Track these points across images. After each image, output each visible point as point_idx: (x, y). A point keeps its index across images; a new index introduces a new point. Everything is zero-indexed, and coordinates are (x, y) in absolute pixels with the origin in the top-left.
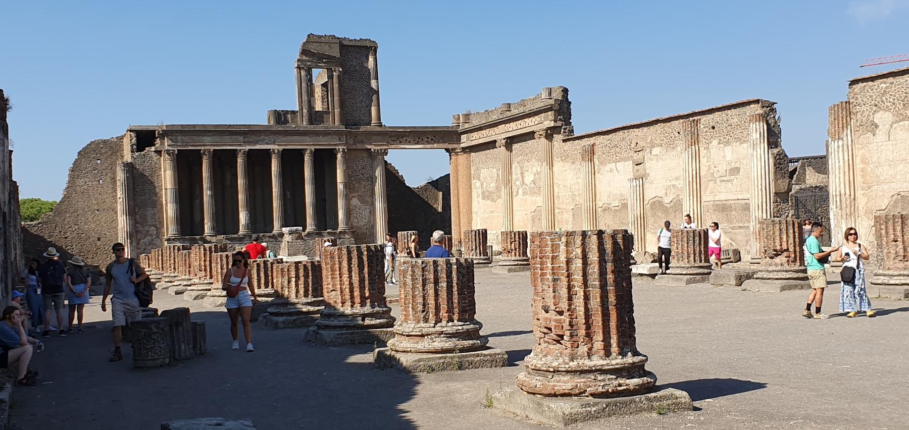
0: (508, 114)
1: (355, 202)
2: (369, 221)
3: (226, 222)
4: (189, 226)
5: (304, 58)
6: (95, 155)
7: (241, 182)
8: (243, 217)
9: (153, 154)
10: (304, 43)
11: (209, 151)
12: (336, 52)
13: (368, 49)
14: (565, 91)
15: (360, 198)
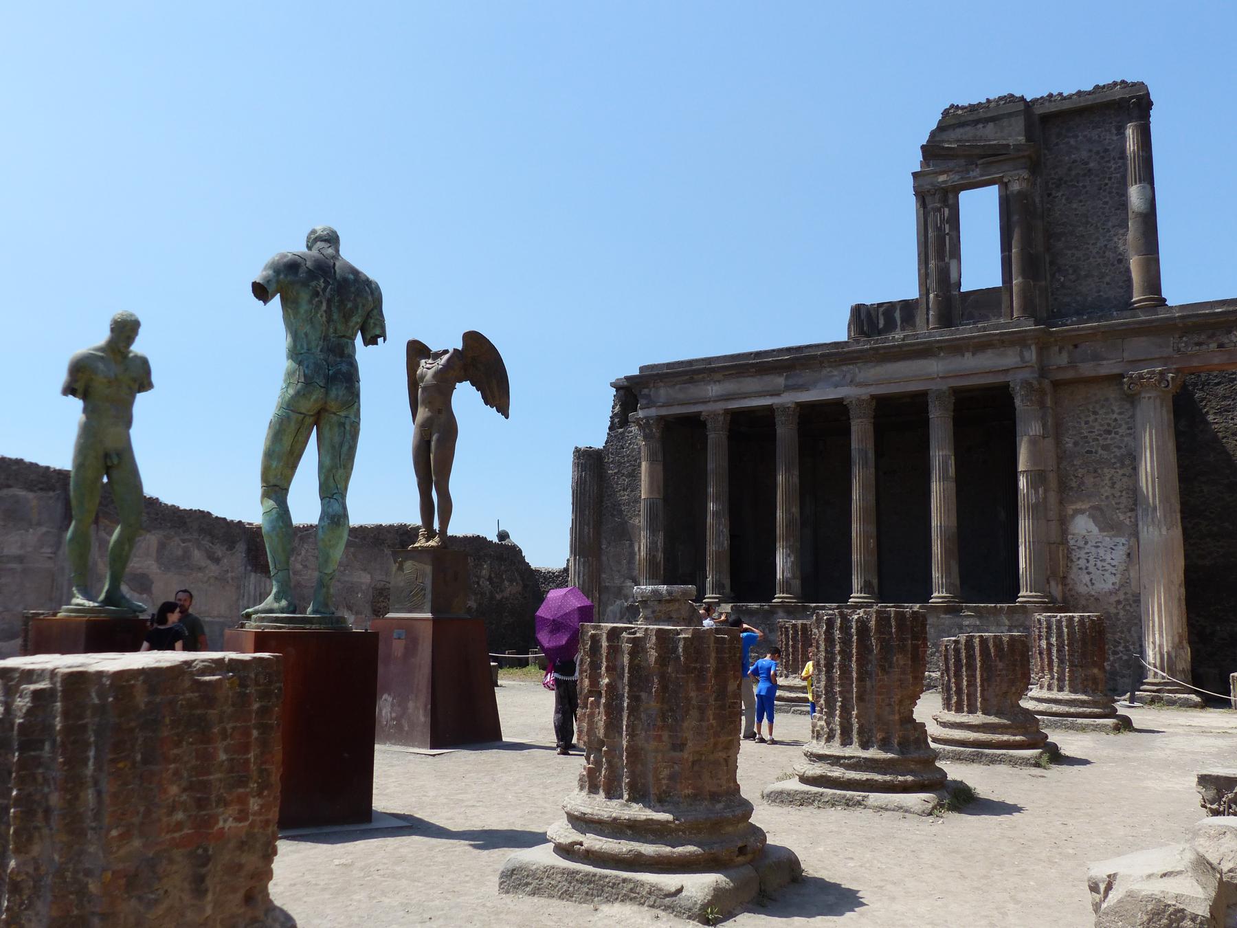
2: (1125, 583)
8: (782, 563)
10: (933, 134)
11: (715, 415)
12: (1014, 135)
13: (1126, 106)
15: (1099, 515)
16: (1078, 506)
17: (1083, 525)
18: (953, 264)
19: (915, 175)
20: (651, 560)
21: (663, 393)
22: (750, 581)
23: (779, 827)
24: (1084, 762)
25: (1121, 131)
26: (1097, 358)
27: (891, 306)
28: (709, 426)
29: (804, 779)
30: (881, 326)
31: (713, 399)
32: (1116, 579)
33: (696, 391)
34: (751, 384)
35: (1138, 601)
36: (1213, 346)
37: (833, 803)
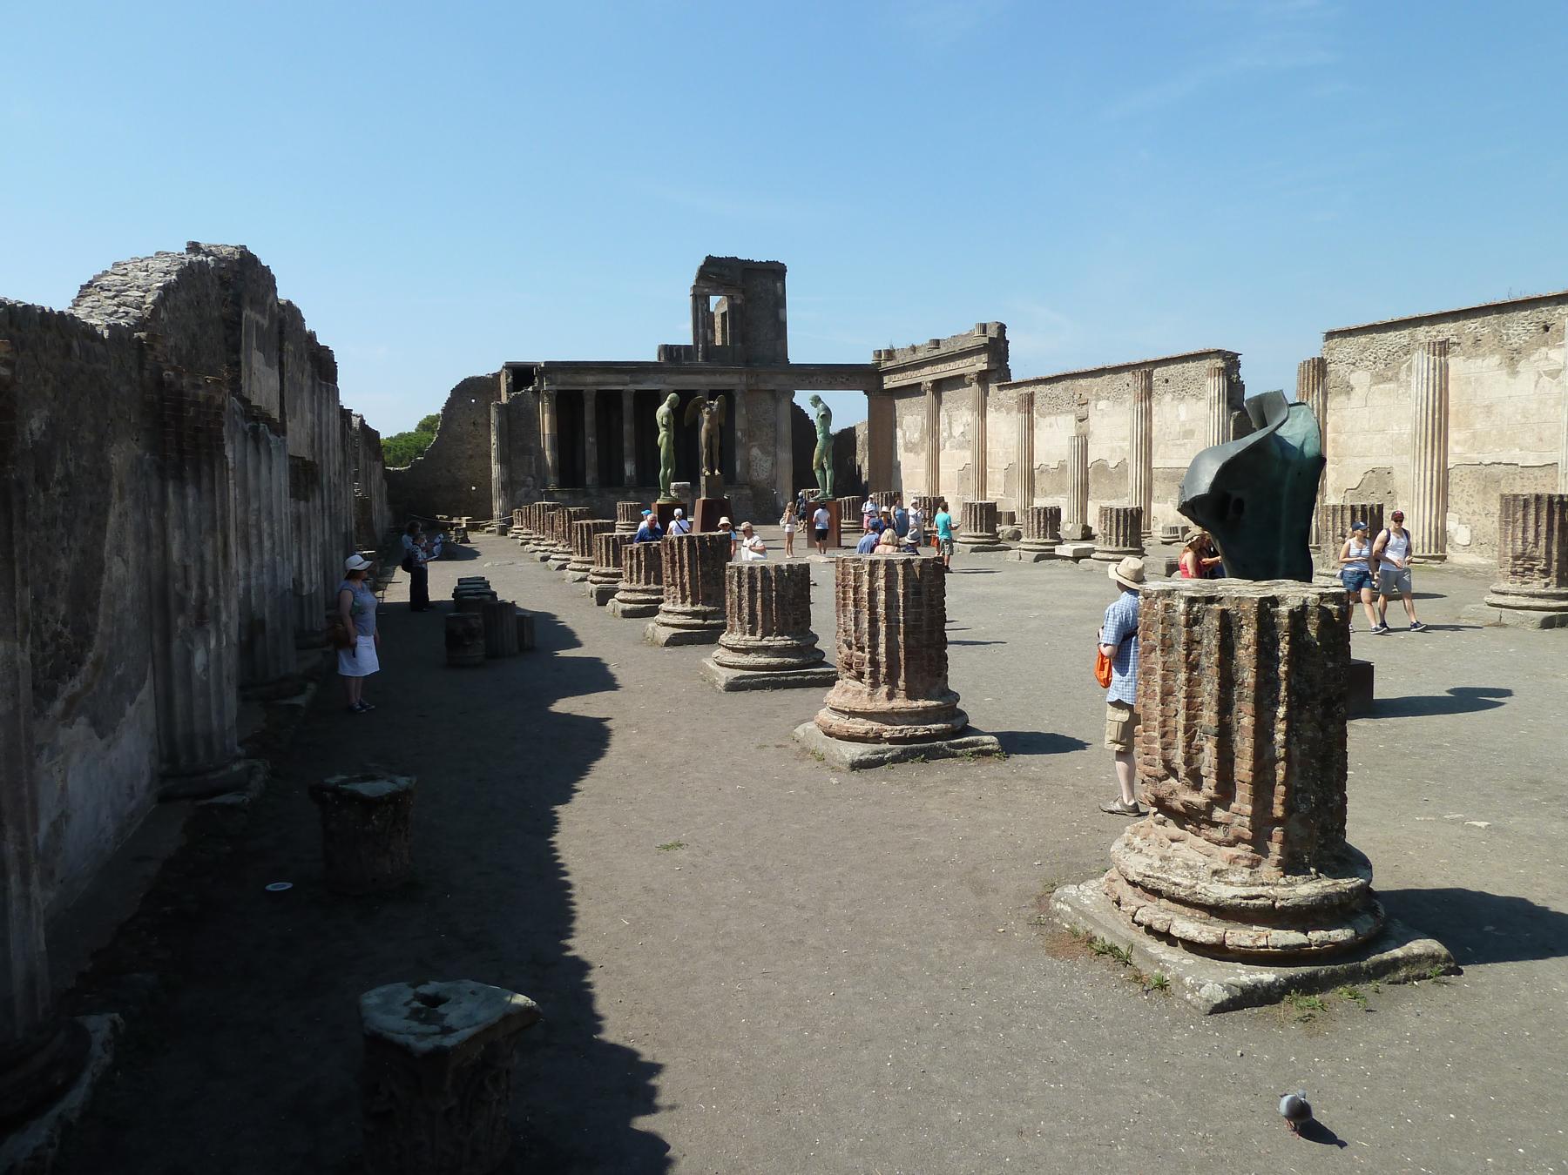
0: (936, 352)
1: (755, 452)
4: (569, 474)
6: (471, 392)
8: (629, 469)
13: (776, 272)
14: (1002, 328)
17: (755, 452)
21: (560, 377)
25: (774, 282)
31: (590, 382)
33: (579, 378)
34: (611, 378)
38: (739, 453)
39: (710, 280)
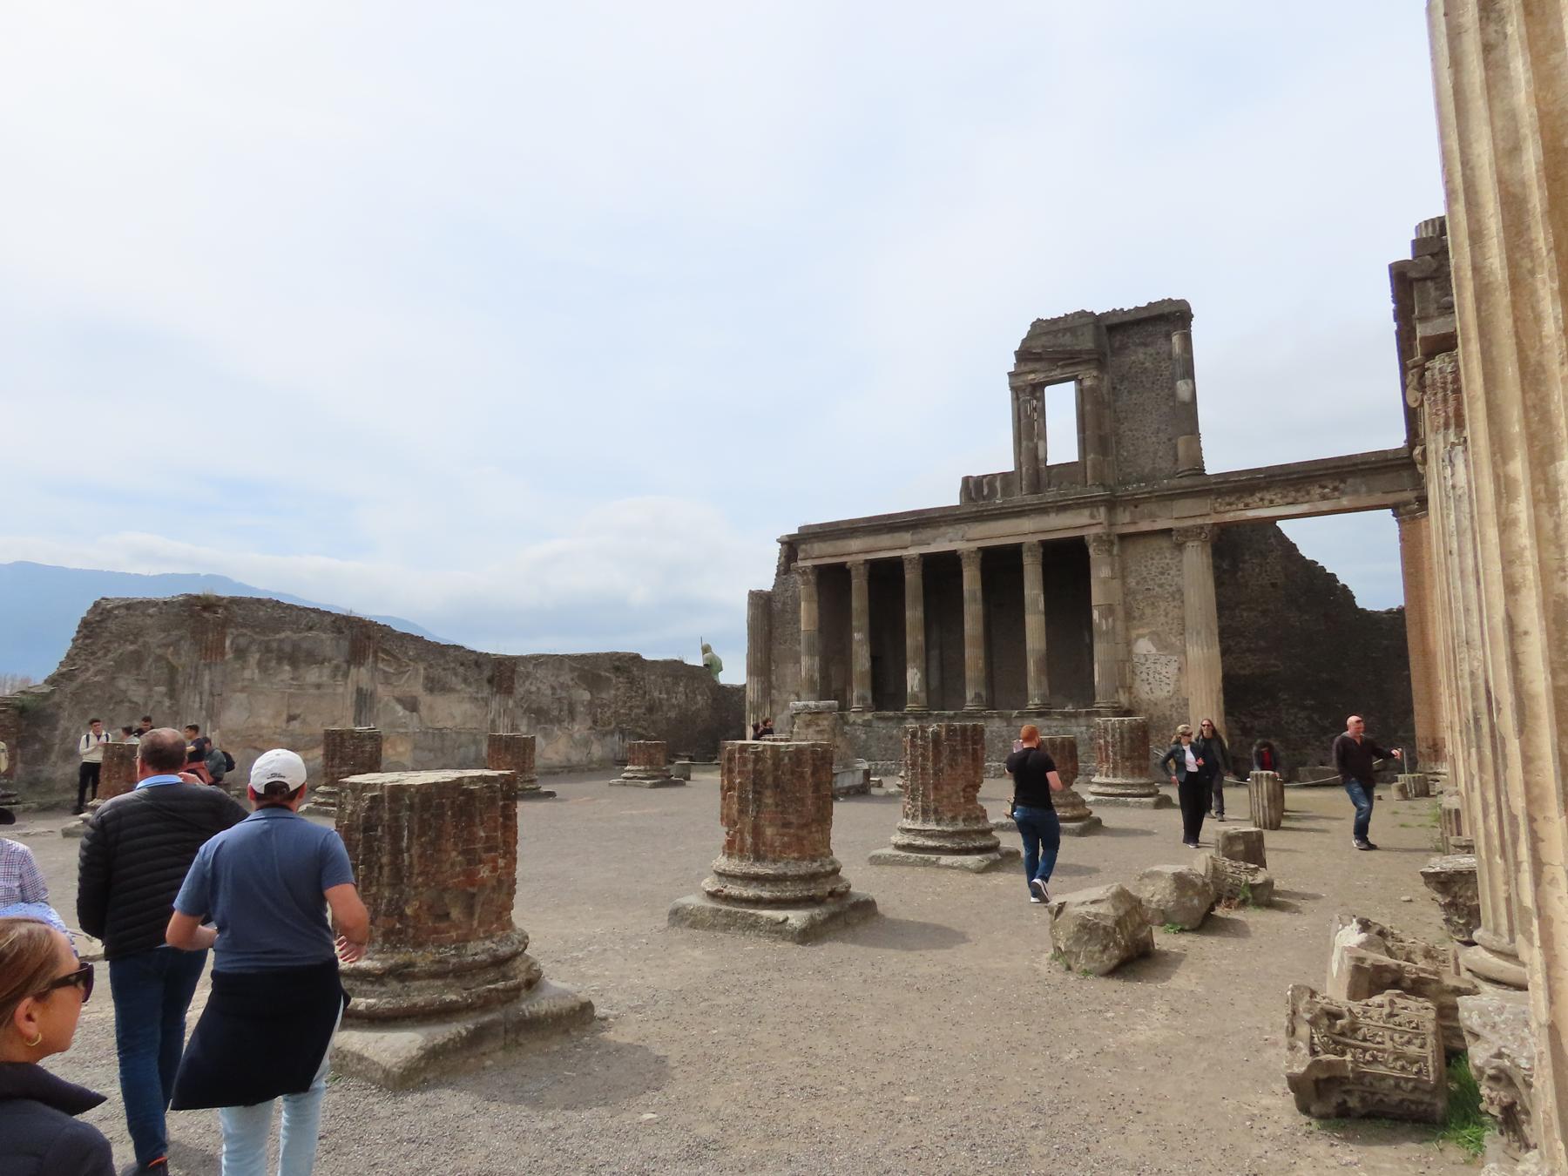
2: (1177, 691)
3: (945, 688)
5: (1024, 368)
7: (908, 614)
8: (913, 678)
9: (797, 577)
10: (1024, 341)
12: (1087, 342)
13: (1171, 319)
15: (1156, 638)
16: (1141, 631)
17: (1144, 646)
18: (1040, 444)
19: (1010, 374)
20: (811, 680)
22: (886, 692)
23: (859, 878)
24: (1149, 833)
25: (1168, 337)
26: (1152, 517)
27: (994, 476)
28: (853, 573)
29: (898, 847)
30: (986, 492)
31: (856, 551)
32: (1171, 688)
34: (885, 540)
35: (1187, 705)
36: (1241, 506)
37: (914, 864)
38: (1100, 649)
39: (1037, 358)
